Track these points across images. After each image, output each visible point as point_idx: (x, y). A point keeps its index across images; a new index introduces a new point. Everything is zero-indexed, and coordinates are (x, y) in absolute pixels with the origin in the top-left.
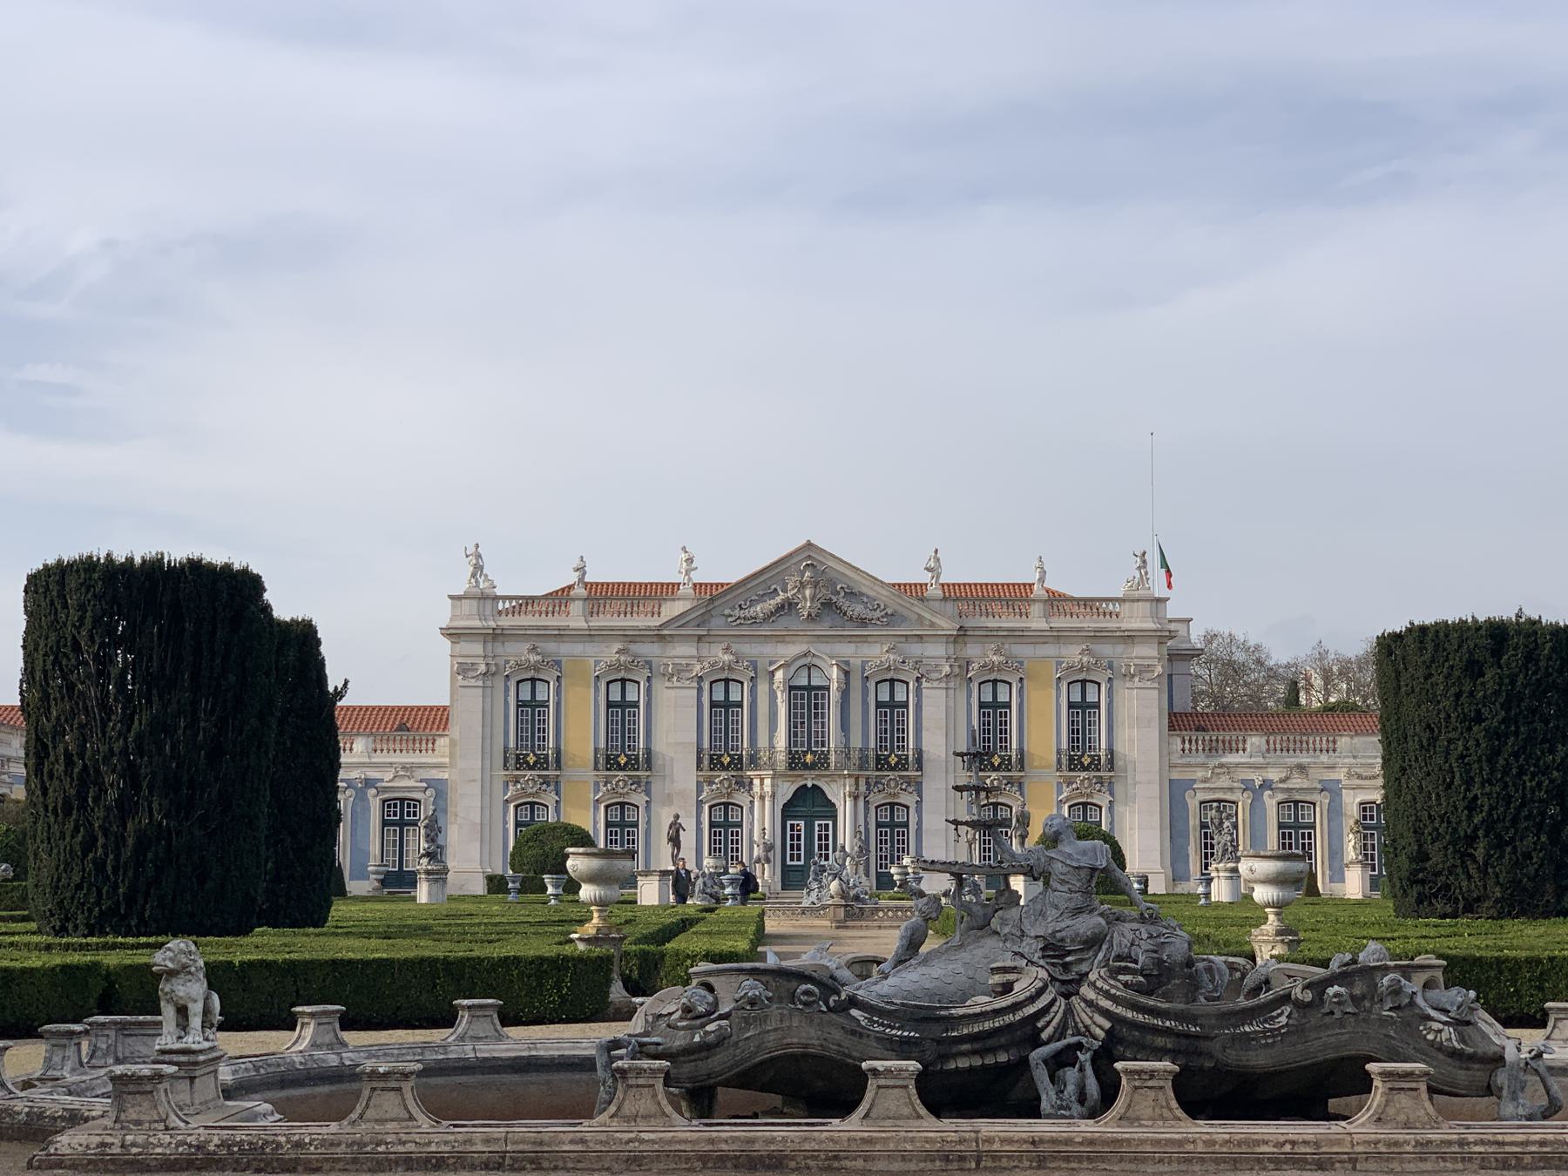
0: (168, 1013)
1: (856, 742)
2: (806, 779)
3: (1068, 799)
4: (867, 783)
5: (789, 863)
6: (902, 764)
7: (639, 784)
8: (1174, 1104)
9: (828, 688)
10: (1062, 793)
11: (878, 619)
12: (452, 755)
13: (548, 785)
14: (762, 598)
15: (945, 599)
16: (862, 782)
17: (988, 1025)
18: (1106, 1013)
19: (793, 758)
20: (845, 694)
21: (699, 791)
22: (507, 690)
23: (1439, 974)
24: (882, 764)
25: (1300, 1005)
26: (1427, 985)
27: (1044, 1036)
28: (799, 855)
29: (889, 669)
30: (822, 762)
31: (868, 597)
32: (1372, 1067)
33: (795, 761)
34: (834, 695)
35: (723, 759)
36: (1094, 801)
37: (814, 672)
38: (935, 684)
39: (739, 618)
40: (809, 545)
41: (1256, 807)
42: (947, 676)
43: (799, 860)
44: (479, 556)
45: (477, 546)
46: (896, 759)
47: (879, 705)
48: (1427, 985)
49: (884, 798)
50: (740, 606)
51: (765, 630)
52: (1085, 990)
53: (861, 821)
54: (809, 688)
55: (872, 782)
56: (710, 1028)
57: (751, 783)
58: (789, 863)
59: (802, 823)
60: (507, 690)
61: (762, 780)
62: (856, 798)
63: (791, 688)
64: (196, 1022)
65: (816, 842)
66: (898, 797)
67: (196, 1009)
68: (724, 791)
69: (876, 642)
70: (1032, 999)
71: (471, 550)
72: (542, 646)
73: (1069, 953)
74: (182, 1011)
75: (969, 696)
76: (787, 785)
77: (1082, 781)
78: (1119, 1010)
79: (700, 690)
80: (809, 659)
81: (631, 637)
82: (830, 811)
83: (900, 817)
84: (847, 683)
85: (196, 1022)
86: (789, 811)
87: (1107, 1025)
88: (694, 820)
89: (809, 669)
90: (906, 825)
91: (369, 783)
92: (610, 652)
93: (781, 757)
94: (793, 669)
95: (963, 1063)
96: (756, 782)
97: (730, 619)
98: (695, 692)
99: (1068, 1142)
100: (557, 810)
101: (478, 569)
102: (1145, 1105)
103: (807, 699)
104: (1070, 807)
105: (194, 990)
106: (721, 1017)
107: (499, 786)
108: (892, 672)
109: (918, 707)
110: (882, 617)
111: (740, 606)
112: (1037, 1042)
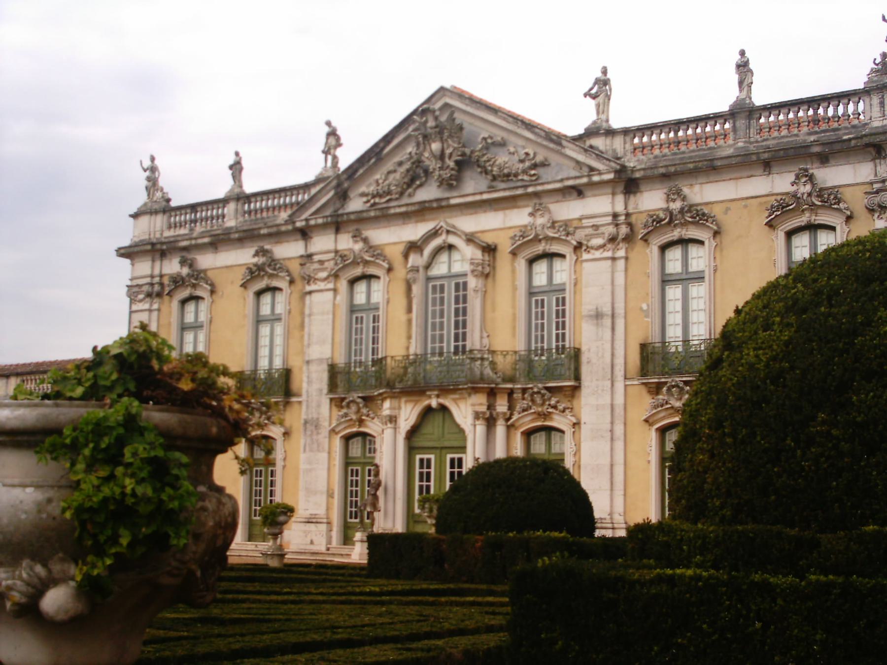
2: (430, 397)
11: (525, 172)
38: (598, 254)
39: (374, 197)
40: (442, 90)
42: (613, 239)
44: (153, 169)
45: (153, 159)
49: (533, 421)
55: (517, 396)
59: (432, 457)
66: (551, 419)
71: (147, 163)
76: (409, 406)
80: (444, 237)
94: (428, 250)
101: (153, 183)
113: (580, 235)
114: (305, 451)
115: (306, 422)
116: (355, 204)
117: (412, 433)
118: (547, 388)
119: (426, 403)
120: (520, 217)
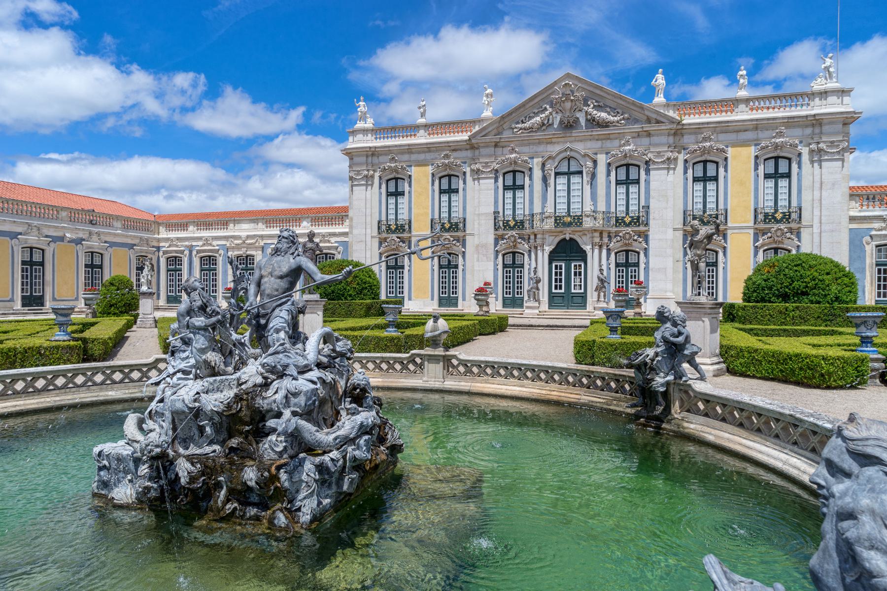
1: (602, 207)
3: (763, 245)
4: (609, 237)
5: (554, 291)
7: (458, 241)
10: (758, 241)
11: (618, 122)
12: (351, 227)
13: (404, 242)
14: (536, 114)
15: (667, 106)
16: (605, 235)
19: (556, 220)
21: (496, 244)
28: (561, 286)
29: (625, 156)
31: (610, 107)
35: (510, 223)
36: (785, 246)
37: (572, 162)
39: (521, 129)
43: (561, 288)
46: (630, 219)
50: (522, 121)
51: (539, 135)
54: (569, 174)
55: (613, 235)
57: (529, 238)
58: (554, 291)
61: (535, 235)
62: (601, 247)
65: (563, 277)
68: (511, 244)
69: (617, 139)
75: (685, 172)
77: (776, 231)
81: (455, 147)
83: (632, 259)
88: (492, 264)
89: (569, 160)
96: (532, 237)
97: (515, 130)
98: (493, 181)
104: (764, 251)
107: (377, 244)
108: (628, 159)
109: (647, 182)
110: (621, 120)
111: (522, 121)
113: (650, 155)
114: (478, 260)
115: (478, 246)
116: (507, 134)
117: (551, 253)
118: (632, 231)
119: (563, 237)
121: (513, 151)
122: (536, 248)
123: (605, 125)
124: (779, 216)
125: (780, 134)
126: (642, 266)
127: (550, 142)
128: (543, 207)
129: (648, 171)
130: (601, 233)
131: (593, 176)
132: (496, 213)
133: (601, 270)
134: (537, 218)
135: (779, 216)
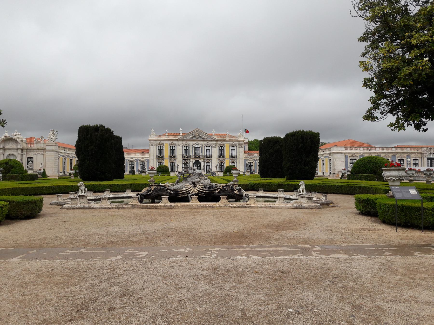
0: (80, 191)
1: (203, 154)
6: (209, 157)
8: (198, 201)
9: (200, 147)
12: (150, 156)
16: (204, 160)
17: (183, 192)
18: (198, 190)
20: (202, 148)
22: (157, 147)
23: (237, 186)
24: (207, 157)
25: (221, 189)
26: (236, 187)
27: (190, 193)
30: (199, 157)
32: (221, 196)
33: (195, 157)
34: (201, 148)
41: (255, 163)
47: (206, 150)
48: (236, 187)
52: (196, 188)
53: (204, 165)
54: (197, 147)
56: (150, 192)
60: (157, 147)
63: (195, 147)
64: (83, 192)
67: (83, 190)
70: (189, 189)
72: (161, 142)
73: (195, 183)
74: (82, 190)
75: (218, 148)
78: (199, 190)
79: (183, 147)
82: (200, 163)
84: (202, 147)
85: (83, 192)
86: (194, 163)
87: (198, 191)
90: (210, 165)
91: (139, 160)
92: (171, 142)
93: (194, 157)
95: (181, 196)
99: (185, 205)
100: (164, 163)
102: (194, 201)
103: (197, 149)
105: (83, 188)
106: (151, 191)
107: (156, 160)
109: (212, 150)
112: (189, 193)
116: (185, 139)
120: (205, 142)
121: (186, 142)
122: (191, 162)
123: (204, 139)
124: (233, 157)
125: (234, 143)
126: (211, 165)
127: (193, 141)
128: (192, 154)
129: (212, 148)
130: (203, 159)
131: (202, 148)
132: (183, 154)
133: (203, 166)
134: (191, 156)
135: (233, 157)
